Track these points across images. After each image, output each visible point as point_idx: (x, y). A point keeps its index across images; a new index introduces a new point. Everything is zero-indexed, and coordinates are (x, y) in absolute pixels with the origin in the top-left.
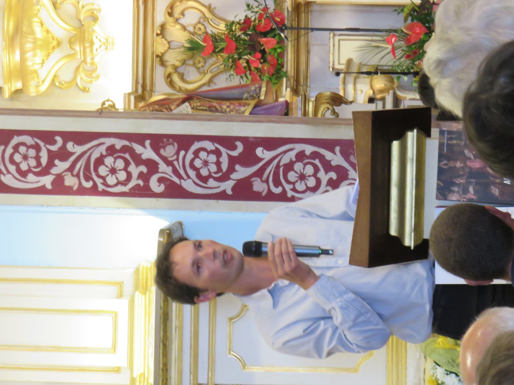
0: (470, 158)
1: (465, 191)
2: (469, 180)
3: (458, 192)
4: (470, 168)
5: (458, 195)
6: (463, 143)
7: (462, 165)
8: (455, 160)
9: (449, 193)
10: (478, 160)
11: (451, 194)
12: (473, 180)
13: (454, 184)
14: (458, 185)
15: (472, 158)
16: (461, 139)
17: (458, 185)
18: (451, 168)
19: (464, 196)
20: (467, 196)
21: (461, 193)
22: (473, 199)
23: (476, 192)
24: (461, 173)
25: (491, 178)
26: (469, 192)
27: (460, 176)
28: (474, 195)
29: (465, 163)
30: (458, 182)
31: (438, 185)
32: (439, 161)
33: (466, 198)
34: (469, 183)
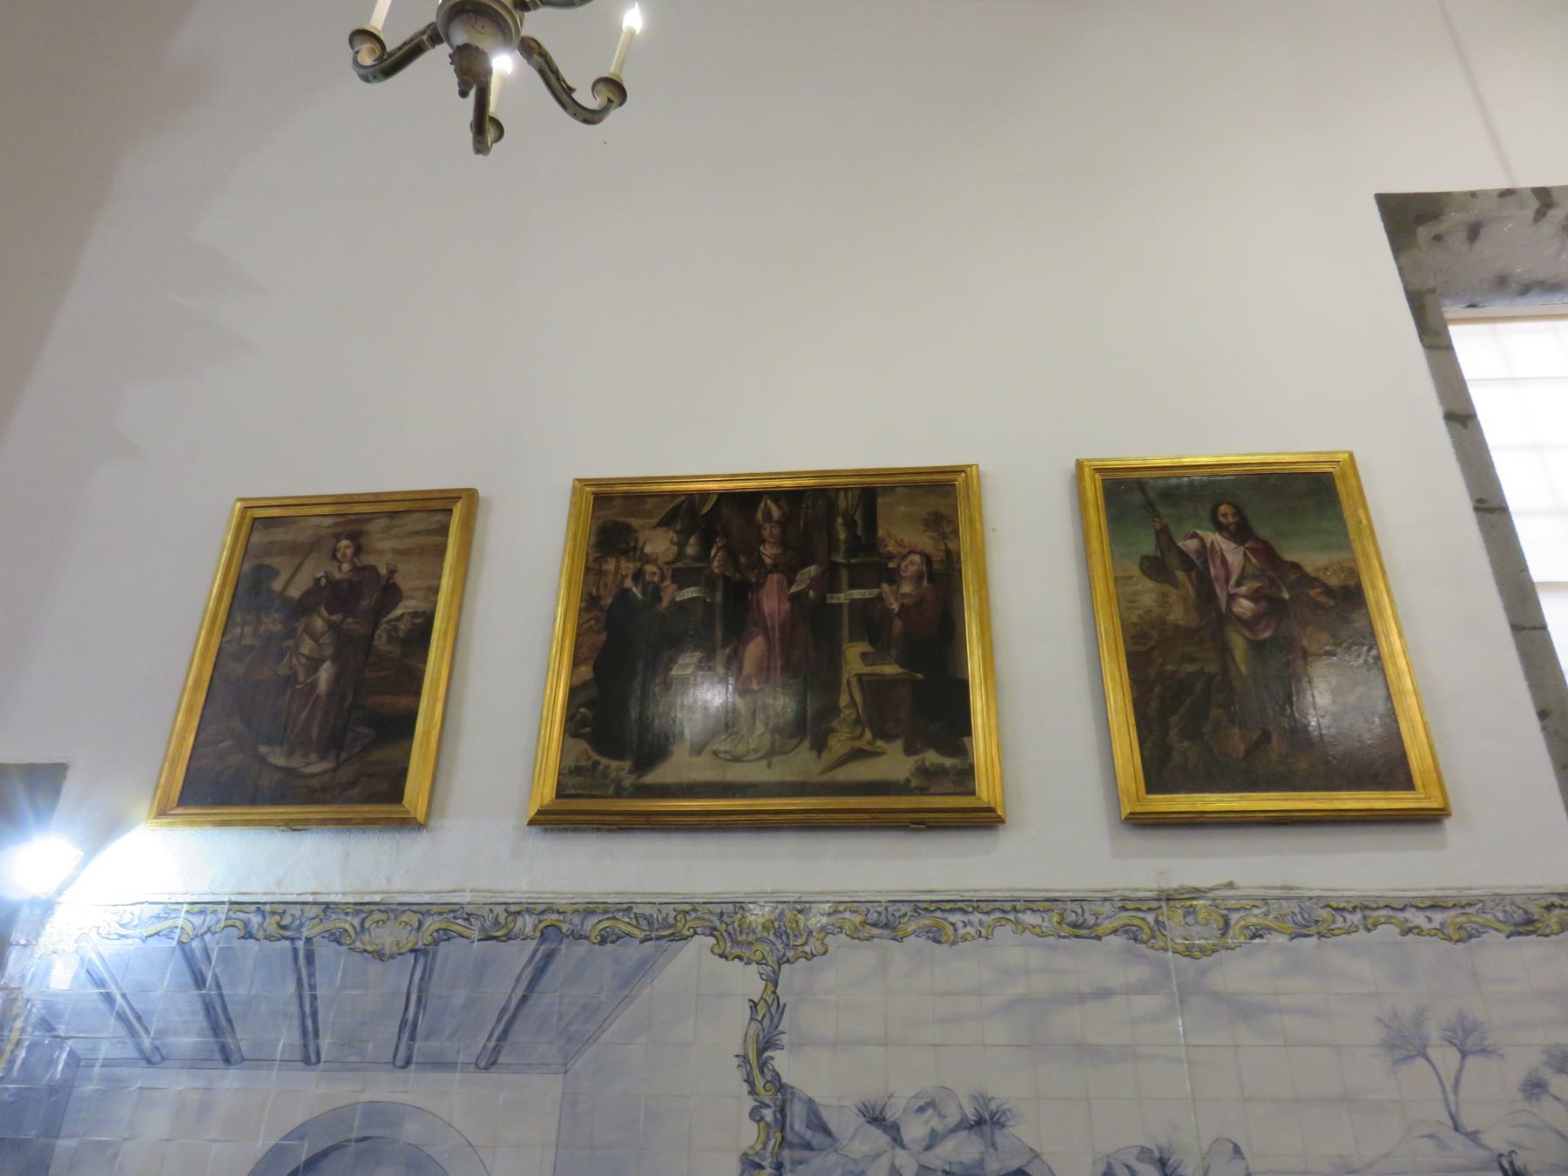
0: (791, 582)
1: (682, 578)
2: (720, 583)
3: (681, 555)
4: (760, 585)
5: (671, 557)
6: (839, 558)
7: (768, 561)
8: (783, 543)
9: (676, 532)
10: (786, 606)
12: (719, 597)
14: (704, 555)
15: (793, 590)
16: (851, 552)
17: (704, 555)
18: (759, 528)
19: (669, 574)
20: (667, 582)
21: (679, 565)
22: (660, 599)
23: (682, 607)
24: (742, 559)
26: (681, 588)
27: (731, 554)
28: (672, 602)
29: (775, 568)
31: (705, 494)
32: (777, 495)
33: (663, 578)
34: (710, 583)
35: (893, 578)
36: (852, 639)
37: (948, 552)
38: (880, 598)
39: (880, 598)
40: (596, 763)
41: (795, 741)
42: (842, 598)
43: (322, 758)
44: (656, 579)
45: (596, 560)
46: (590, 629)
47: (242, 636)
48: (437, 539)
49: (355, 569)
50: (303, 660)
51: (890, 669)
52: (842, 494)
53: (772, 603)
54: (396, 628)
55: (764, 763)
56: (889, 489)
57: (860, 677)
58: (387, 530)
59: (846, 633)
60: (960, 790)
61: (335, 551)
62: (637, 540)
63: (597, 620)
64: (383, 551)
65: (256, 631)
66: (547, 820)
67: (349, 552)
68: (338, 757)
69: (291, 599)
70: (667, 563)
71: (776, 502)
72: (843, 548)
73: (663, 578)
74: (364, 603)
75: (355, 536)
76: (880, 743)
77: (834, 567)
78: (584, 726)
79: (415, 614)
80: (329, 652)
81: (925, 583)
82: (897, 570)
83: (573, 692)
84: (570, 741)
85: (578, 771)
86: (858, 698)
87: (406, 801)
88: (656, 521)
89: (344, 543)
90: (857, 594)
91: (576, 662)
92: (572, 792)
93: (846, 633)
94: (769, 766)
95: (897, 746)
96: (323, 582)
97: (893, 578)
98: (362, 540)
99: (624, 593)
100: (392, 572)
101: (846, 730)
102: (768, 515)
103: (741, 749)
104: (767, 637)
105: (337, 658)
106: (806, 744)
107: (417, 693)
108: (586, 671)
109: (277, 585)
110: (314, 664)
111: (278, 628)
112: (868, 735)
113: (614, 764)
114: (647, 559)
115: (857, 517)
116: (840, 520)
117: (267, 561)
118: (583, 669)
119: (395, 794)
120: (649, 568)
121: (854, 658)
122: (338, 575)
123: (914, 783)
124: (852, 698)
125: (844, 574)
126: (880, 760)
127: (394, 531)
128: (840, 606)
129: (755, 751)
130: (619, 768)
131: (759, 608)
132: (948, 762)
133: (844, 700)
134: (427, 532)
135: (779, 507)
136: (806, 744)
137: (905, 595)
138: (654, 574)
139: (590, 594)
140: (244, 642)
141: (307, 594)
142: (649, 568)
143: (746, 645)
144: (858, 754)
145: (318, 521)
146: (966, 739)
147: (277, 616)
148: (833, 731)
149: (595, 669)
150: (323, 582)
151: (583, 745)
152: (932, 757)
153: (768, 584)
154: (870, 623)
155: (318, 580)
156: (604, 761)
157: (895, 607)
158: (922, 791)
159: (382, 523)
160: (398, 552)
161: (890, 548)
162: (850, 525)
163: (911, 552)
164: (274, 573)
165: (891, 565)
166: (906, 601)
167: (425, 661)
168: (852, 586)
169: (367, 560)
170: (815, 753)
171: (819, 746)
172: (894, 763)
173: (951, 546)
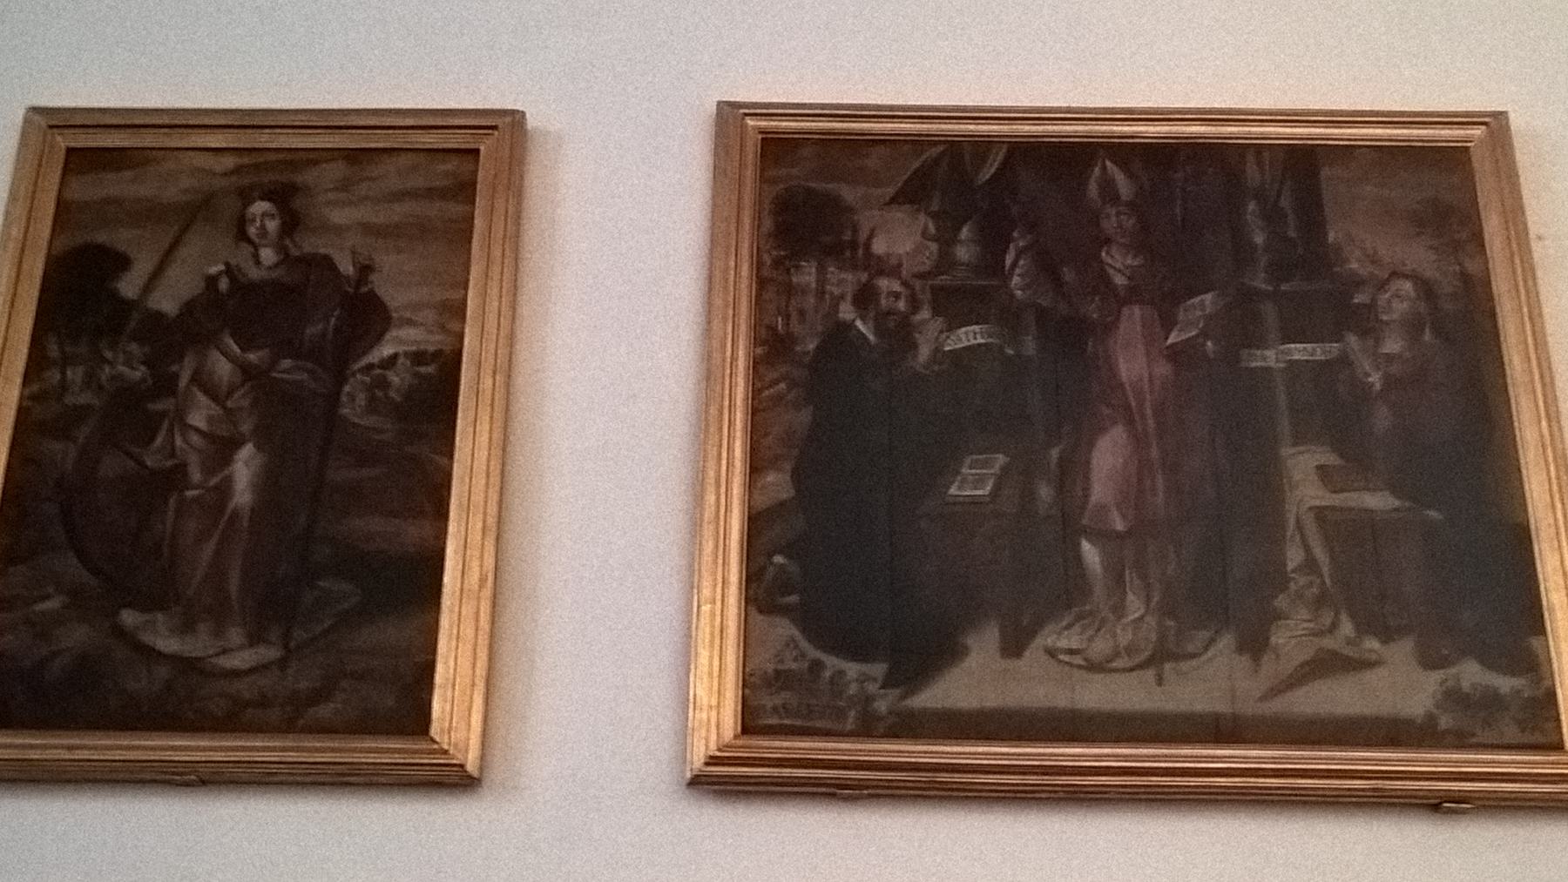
0: (1168, 324)
1: (956, 304)
3: (945, 262)
4: (1109, 328)
5: (927, 265)
6: (1260, 282)
7: (1119, 280)
8: (1141, 243)
9: (935, 216)
10: (1163, 369)
11: (932, 229)
12: (1030, 346)
13: (994, 240)
16: (1280, 270)
17: (992, 264)
20: (925, 314)
21: (943, 280)
22: (914, 346)
24: (1068, 275)
25: (1055, 453)
26: (951, 327)
27: (1047, 267)
30: (1008, 261)
31: (984, 145)
33: (915, 305)
34: (1009, 318)
35: (1366, 323)
36: (1298, 439)
37: (1465, 278)
38: (1344, 361)
39: (1344, 361)
40: (816, 666)
41: (1204, 635)
42: (1270, 357)
43: (254, 639)
44: (902, 305)
45: (777, 263)
46: (779, 398)
47: (64, 386)
48: (455, 209)
49: (286, 259)
50: (195, 439)
51: (1378, 501)
52: (1250, 158)
53: (1133, 360)
54: (383, 384)
55: (1150, 674)
56: (1345, 153)
57: (1320, 513)
58: (345, 186)
59: (1284, 425)
60: (1538, 738)
61: (242, 222)
62: (855, 231)
63: (793, 384)
64: (342, 226)
65: (90, 380)
66: (720, 781)
67: (272, 225)
68: (286, 636)
69: (159, 316)
70: (921, 276)
71: (1124, 165)
72: (1263, 261)
73: (915, 305)
74: (311, 330)
75: (284, 197)
76: (1372, 644)
77: (1248, 297)
78: (787, 589)
79: (418, 358)
80: (246, 427)
81: (1427, 336)
82: (1371, 306)
83: (756, 523)
84: (758, 619)
85: (780, 679)
86: (1320, 553)
87: (434, 730)
88: (890, 191)
89: (260, 207)
90: (1299, 351)
91: (756, 467)
92: (774, 721)
93: (1284, 425)
94: (1160, 681)
95: (1402, 652)
96: (224, 284)
97: (1366, 323)
98: (298, 203)
99: (839, 334)
100: (365, 270)
101: (1304, 613)
102: (1109, 191)
103: (1100, 647)
104: (1130, 423)
105: (262, 437)
106: (1226, 641)
107: (442, 515)
108: (778, 484)
109: (129, 286)
110: (223, 449)
111: (138, 373)
112: (1347, 628)
113: (852, 669)
114: (882, 267)
115: (1285, 202)
116: (1252, 206)
117: (102, 237)
118: (771, 477)
119: (416, 720)
120: (884, 283)
121: (1306, 479)
122: (254, 274)
123: (1445, 722)
124: (1307, 549)
125: (1269, 310)
126: (1370, 676)
127: (363, 189)
128: (1267, 369)
129: (1130, 650)
130: (858, 674)
131: (1113, 372)
132: (1505, 684)
133: (1294, 557)
134: (430, 193)
135: (1130, 175)
136: (1226, 641)
137: (1390, 358)
138: (897, 296)
139: (772, 328)
140: (69, 400)
141: (189, 307)
142: (884, 283)
143: (1091, 444)
144: (1326, 665)
145: (202, 160)
146: (1535, 642)
147: (134, 347)
148: (1279, 616)
149: (797, 476)
150: (224, 284)
151: (784, 629)
152: (1471, 674)
153: (1124, 325)
154: (1332, 409)
155: (212, 281)
156: (832, 662)
157: (1375, 379)
158: (1461, 741)
159: (337, 170)
160: (368, 229)
161: (1354, 266)
162: (1272, 216)
163: (1395, 274)
164: (122, 263)
165: (1359, 298)
166: (1394, 369)
167: (450, 456)
168: (1291, 335)
169: (310, 244)
170: (1244, 661)
171: (1254, 645)
172: (1400, 683)
173: (1472, 267)
